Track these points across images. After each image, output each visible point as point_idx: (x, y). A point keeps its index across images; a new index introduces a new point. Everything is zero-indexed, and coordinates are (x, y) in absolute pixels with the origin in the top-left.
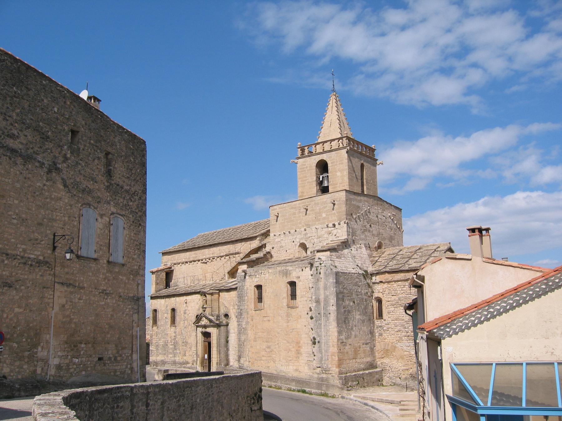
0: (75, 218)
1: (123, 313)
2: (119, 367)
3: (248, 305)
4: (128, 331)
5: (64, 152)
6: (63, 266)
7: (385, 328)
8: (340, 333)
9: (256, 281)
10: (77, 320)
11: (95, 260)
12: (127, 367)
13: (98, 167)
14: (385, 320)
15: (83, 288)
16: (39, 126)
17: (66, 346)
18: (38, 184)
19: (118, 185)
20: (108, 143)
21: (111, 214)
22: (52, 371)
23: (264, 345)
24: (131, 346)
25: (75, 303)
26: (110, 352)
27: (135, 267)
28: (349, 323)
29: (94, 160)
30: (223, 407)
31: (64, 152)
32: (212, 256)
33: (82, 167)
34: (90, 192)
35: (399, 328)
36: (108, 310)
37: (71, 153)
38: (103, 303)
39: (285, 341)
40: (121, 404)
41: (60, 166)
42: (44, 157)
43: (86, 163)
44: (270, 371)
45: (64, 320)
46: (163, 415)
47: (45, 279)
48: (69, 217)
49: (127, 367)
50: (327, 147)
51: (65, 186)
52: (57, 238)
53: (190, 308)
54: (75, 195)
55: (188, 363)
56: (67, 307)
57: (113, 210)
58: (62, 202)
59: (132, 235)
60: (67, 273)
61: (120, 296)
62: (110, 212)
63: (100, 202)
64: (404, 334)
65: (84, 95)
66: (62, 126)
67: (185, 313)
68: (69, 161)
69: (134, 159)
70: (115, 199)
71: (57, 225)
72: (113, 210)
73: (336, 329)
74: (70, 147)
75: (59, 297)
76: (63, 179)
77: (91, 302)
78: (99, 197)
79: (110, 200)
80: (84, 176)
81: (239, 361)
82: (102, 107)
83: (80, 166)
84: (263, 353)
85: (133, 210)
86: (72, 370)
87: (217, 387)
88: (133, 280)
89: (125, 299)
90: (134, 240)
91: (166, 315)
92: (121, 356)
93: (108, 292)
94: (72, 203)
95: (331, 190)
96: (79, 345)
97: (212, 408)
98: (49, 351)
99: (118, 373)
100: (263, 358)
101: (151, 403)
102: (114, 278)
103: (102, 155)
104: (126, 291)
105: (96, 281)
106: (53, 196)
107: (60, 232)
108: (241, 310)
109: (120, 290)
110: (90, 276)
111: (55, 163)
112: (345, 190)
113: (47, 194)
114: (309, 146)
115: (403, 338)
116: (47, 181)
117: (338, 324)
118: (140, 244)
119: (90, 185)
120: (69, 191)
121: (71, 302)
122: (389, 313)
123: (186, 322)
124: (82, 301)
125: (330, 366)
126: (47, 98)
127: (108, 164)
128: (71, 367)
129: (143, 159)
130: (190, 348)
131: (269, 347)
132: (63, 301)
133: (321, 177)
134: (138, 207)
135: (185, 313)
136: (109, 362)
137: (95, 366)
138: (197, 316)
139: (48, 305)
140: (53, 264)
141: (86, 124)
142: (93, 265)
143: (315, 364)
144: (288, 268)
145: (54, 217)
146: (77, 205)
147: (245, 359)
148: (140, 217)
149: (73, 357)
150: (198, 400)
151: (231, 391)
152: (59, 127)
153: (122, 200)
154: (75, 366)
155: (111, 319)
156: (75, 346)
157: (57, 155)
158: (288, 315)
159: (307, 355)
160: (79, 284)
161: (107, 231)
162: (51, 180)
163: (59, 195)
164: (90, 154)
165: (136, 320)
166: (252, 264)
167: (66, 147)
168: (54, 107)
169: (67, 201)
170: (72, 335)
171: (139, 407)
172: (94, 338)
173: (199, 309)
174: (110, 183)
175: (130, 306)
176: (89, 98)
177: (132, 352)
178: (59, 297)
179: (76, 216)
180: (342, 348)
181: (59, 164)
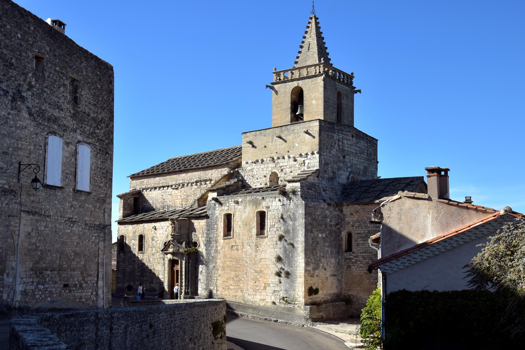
0: (41, 146)
1: (89, 241)
2: (84, 294)
3: (217, 234)
4: (94, 259)
5: (28, 80)
6: (28, 194)
7: (353, 261)
8: (307, 264)
10: (43, 248)
11: (61, 188)
12: (92, 294)
13: (64, 94)
14: (353, 253)
15: (49, 216)
16: (2, 53)
17: (31, 272)
18: (3, 113)
19: (84, 113)
20: (74, 69)
21: (77, 143)
22: (18, 297)
23: (233, 274)
24: (96, 273)
25: (41, 231)
26: (75, 279)
27: (102, 196)
29: (59, 87)
30: (184, 333)
31: (28, 80)
32: (181, 182)
33: (48, 94)
34: (56, 120)
35: (367, 261)
36: (73, 238)
37: (36, 80)
38: (69, 231)
39: (253, 271)
40: (86, 328)
41: (24, 94)
42: (8, 86)
43: (52, 90)
44: (237, 300)
45: (30, 247)
46: (126, 339)
47: (11, 207)
48: (35, 145)
49: (92, 294)
51: (30, 114)
52: (22, 167)
54: (40, 124)
55: (156, 291)
56: (33, 234)
57: (79, 138)
58: (27, 131)
59: (99, 163)
60: (33, 201)
61: (86, 224)
62: (76, 140)
63: (66, 130)
65: (49, 21)
66: (26, 53)
67: (153, 240)
68: (34, 89)
69: (101, 85)
70: (82, 127)
71: (22, 154)
72: (79, 138)
73: (303, 260)
74: (34, 74)
75: (24, 225)
76: (28, 107)
77: (58, 230)
78: (65, 125)
79: (76, 128)
80: (50, 104)
82: (68, 33)
83: (45, 94)
84: (231, 282)
85: (100, 138)
86: (38, 296)
87: (179, 314)
88: (99, 208)
89: (91, 227)
90: (101, 168)
91: (133, 241)
92: (86, 283)
93: (74, 220)
94: (38, 131)
95: (305, 118)
96: (45, 272)
97: (173, 334)
98: (15, 278)
99: (84, 300)
100: (231, 287)
101: (115, 327)
102: (80, 206)
103: (67, 83)
104: (92, 219)
105: (62, 209)
106: (18, 125)
107: (25, 161)
108: (210, 238)
109: (87, 218)
110: (56, 204)
111: (19, 92)
112: (319, 120)
113: (12, 122)
114: (285, 71)
116: (12, 109)
117: (306, 254)
118: (107, 172)
119: (56, 113)
120: (35, 120)
121: (36, 230)
122: (358, 245)
123: (153, 249)
124: (48, 229)
125: (297, 296)
126: (9, 23)
127: (75, 91)
128: (36, 293)
129: (110, 85)
132: (30, 229)
134: (105, 135)
135: (153, 240)
136: (74, 289)
137: (60, 292)
138: (166, 243)
139: (14, 233)
140: (19, 192)
141: (51, 50)
142: (60, 194)
145: (20, 146)
146: (42, 134)
148: (107, 144)
149: (39, 283)
150: (161, 326)
151: (194, 318)
152: (23, 54)
153: (88, 128)
154: (40, 293)
155: (77, 246)
156: (40, 273)
157: (22, 83)
158: (257, 246)
159: (274, 285)
160: (45, 212)
161: (73, 160)
162: (16, 109)
163: (25, 124)
164: (55, 81)
165: (102, 248)
167: (30, 75)
168: (17, 33)
169: (32, 129)
170: (37, 262)
171: (103, 331)
172: (59, 265)
173: (167, 236)
174: (76, 111)
175: (96, 234)
176: (53, 22)
177: (98, 278)
178: (24, 225)
179: (42, 145)
180: (309, 278)
181: (24, 92)
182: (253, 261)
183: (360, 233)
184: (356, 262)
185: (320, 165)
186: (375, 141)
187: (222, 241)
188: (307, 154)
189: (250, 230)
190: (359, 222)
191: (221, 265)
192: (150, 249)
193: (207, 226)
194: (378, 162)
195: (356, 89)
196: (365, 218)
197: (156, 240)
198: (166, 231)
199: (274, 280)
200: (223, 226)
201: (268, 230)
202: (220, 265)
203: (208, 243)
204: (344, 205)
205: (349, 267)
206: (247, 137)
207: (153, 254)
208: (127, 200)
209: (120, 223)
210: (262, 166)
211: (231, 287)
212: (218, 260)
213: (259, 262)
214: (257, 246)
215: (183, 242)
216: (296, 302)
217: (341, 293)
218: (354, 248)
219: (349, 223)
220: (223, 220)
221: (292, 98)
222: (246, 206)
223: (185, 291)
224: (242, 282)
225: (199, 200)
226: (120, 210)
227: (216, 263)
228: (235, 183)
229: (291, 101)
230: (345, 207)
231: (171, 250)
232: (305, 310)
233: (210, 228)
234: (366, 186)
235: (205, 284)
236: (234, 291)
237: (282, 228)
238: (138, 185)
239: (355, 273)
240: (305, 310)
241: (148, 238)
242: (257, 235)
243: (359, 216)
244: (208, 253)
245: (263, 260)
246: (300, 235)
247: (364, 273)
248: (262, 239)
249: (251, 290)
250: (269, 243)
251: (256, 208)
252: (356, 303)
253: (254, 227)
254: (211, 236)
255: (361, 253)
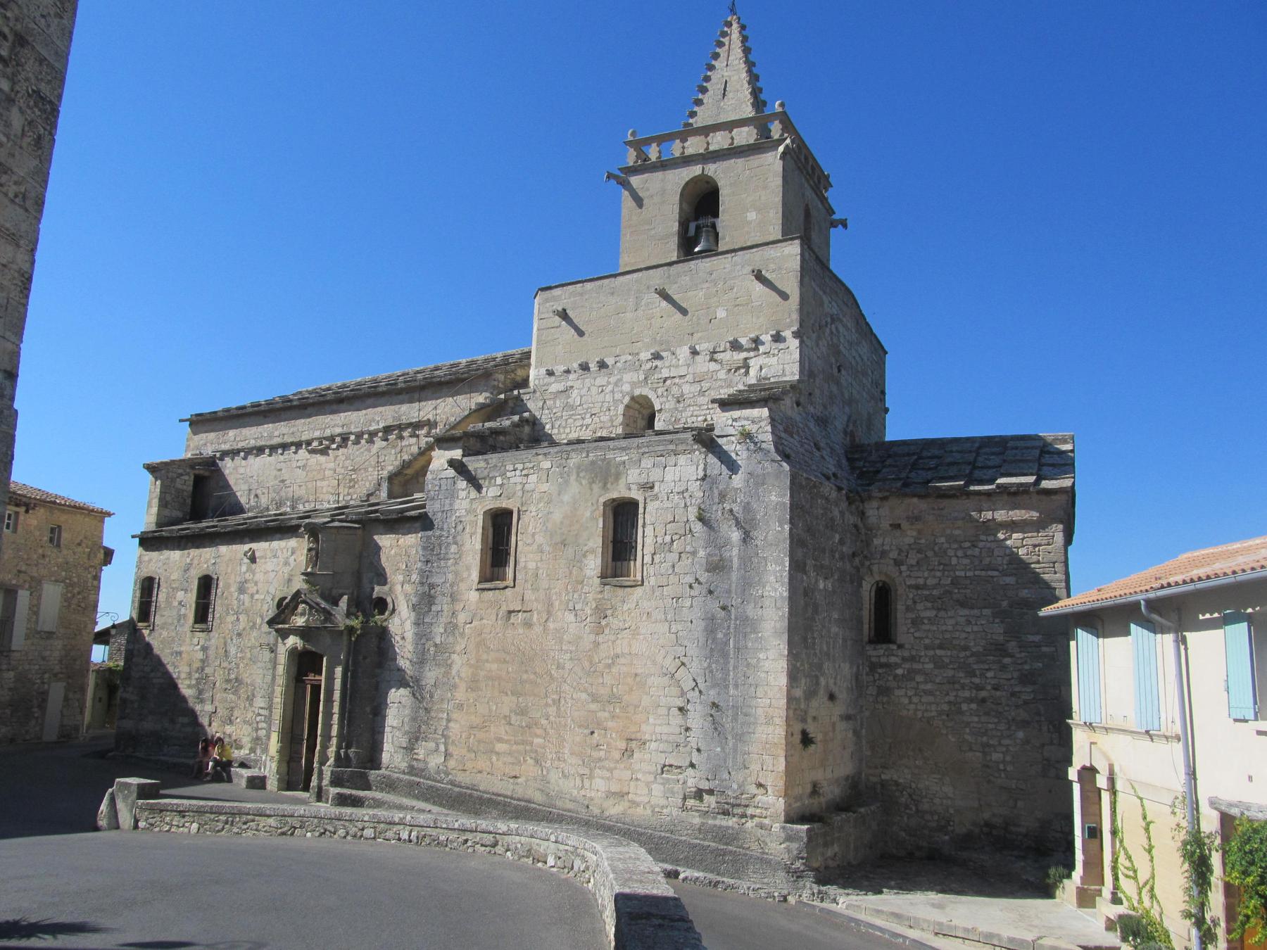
3: (456, 573)
7: (899, 671)
8: (793, 676)
9: (491, 497)
14: (900, 646)
23: (507, 704)
28: (814, 644)
32: (338, 430)
35: (950, 673)
39: (584, 696)
44: (520, 792)
50: (719, 141)
53: (259, 577)
64: (967, 694)
67: (242, 590)
73: (783, 664)
81: (410, 749)
100: (500, 747)
108: (432, 586)
115: (964, 707)
123: (242, 617)
130: (250, 699)
131: (522, 712)
133: (692, 226)
135: (242, 590)
143: (693, 780)
144: (610, 456)
147: (432, 745)
158: (601, 613)
159: (662, 746)
166: (483, 443)
173: (289, 580)
182: (586, 664)
183: (925, 587)
184: (911, 674)
185: (801, 372)
186: (880, 351)
187: (474, 596)
188: (757, 341)
189: (577, 561)
190: (919, 551)
191: (466, 672)
192: (231, 618)
193: (424, 548)
194: (887, 410)
195: (834, 217)
196: (943, 540)
197: (251, 588)
198: (286, 563)
199: (665, 729)
200: (478, 546)
201: (647, 559)
202: (463, 675)
203: (425, 602)
204: (870, 498)
205: (884, 691)
206: (555, 299)
207: (239, 635)
208: (173, 480)
209: (149, 542)
210: (601, 380)
211: (500, 747)
212: (454, 656)
213: (609, 666)
214: (601, 613)
215: (341, 596)
216: (750, 811)
217: (860, 773)
218: (902, 629)
219: (884, 554)
220: (480, 531)
221: (681, 209)
222: (567, 482)
223: (338, 753)
224: (539, 732)
225: (391, 478)
226: (150, 506)
227: (450, 666)
228: (515, 425)
229: (680, 217)
230: (875, 504)
231: (300, 621)
232: (789, 838)
233: (432, 555)
234: (908, 455)
235: (406, 733)
236: (510, 760)
237: (702, 553)
238: (209, 444)
239: (904, 713)
240: (789, 838)
241: (228, 586)
242: (603, 576)
243: (920, 532)
244: (423, 636)
245: (622, 661)
246: (772, 579)
247: (940, 713)
248: (620, 592)
249: (574, 760)
250: (646, 605)
251: (604, 487)
252: (907, 807)
253: (593, 551)
254: (436, 580)
255: (927, 648)
